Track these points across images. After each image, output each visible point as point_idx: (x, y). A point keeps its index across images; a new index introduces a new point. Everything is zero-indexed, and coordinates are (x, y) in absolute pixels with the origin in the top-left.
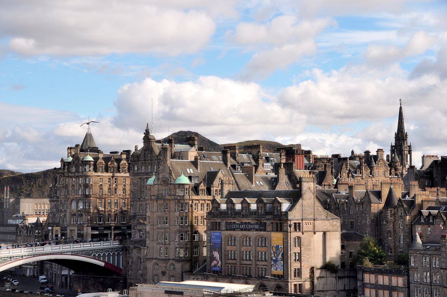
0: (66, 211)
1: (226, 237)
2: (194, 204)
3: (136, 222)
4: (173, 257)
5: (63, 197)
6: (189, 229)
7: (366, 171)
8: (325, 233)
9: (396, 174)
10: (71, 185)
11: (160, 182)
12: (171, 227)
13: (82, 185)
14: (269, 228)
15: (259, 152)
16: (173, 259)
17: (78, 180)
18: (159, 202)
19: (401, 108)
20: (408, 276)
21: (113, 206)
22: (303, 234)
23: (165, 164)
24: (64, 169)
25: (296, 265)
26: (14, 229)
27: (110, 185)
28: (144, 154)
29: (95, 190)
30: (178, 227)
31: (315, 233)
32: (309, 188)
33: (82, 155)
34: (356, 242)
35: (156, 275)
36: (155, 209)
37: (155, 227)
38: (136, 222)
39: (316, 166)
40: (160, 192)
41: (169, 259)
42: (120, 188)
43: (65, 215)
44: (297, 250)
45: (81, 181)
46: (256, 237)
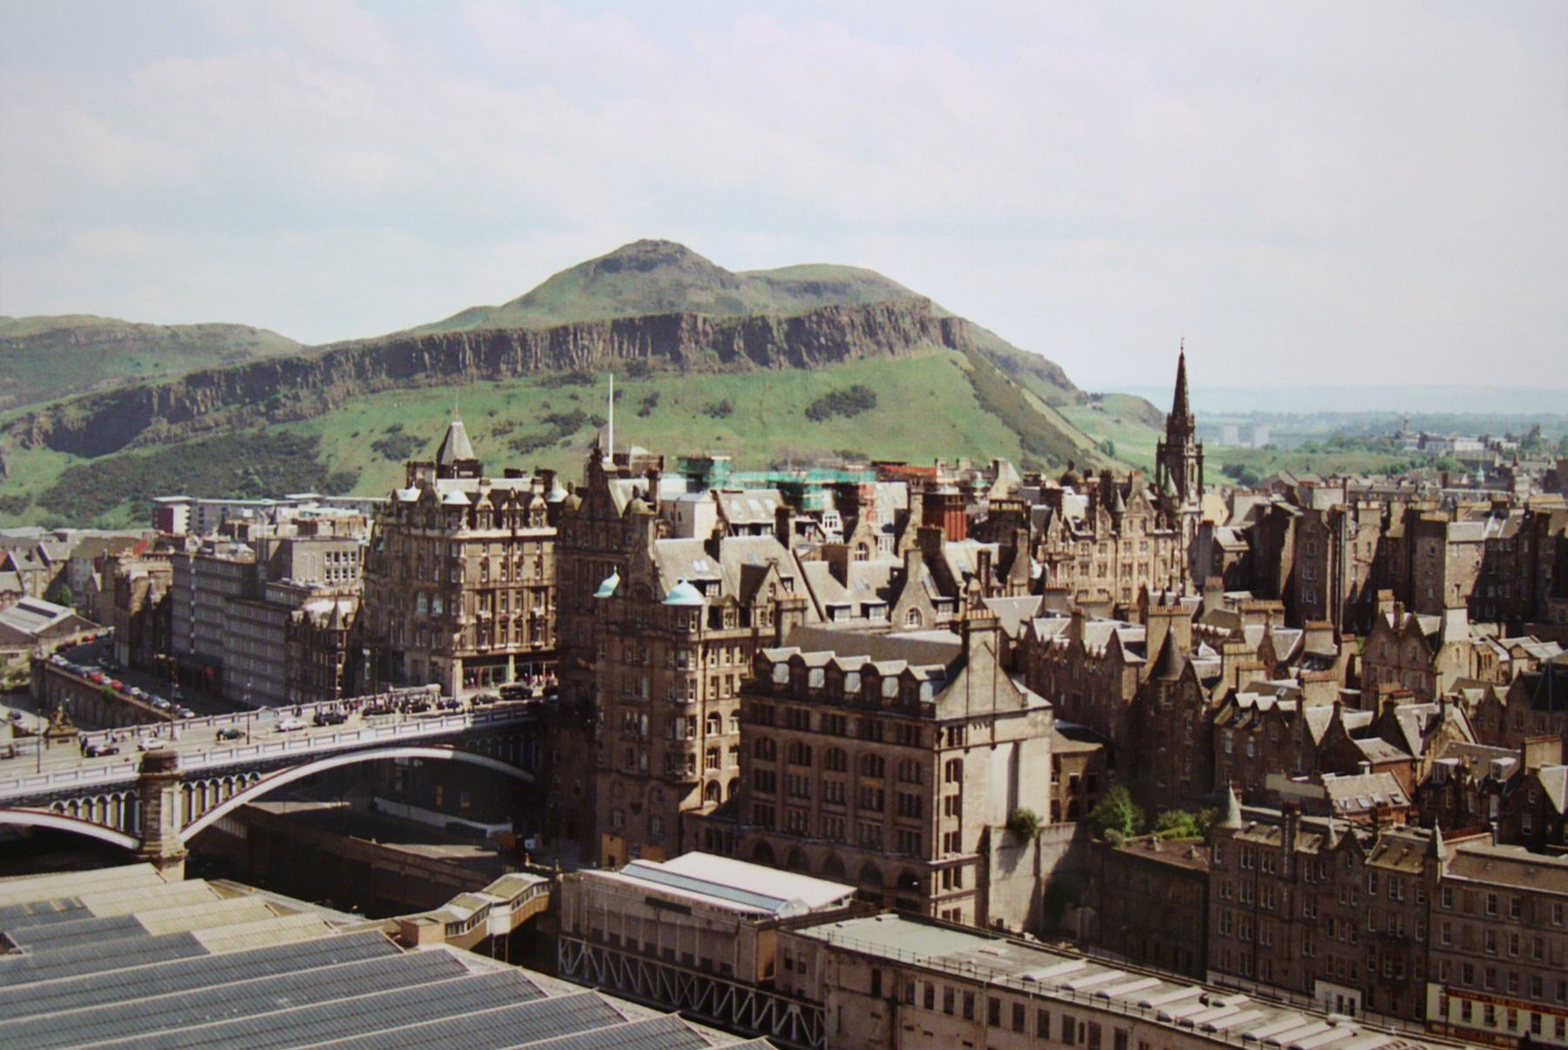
0: (402, 615)
7: (1102, 527)
8: (1017, 744)
9: (1170, 526)
10: (414, 556)
14: (889, 735)
16: (658, 778)
18: (627, 642)
21: (512, 607)
25: (948, 825)
27: (506, 558)
32: (985, 644)
36: (617, 655)
37: (617, 699)
41: (650, 777)
42: (529, 562)
43: (401, 625)
44: (951, 789)
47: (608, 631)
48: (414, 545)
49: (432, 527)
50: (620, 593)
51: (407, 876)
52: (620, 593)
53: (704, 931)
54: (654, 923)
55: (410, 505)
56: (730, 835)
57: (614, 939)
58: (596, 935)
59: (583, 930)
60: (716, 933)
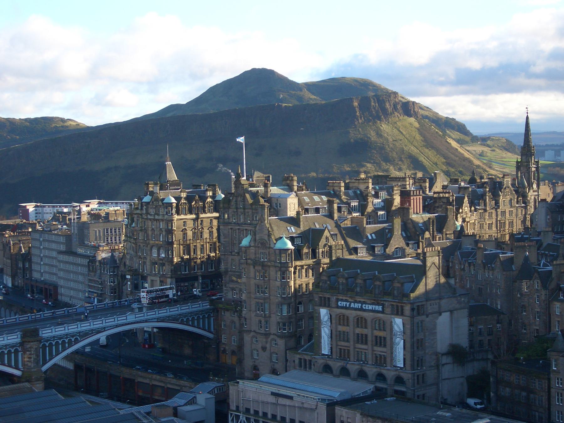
0: (145, 258)
1: (337, 315)
2: (297, 270)
3: (227, 279)
4: (275, 332)
5: (141, 241)
6: (293, 300)
10: (150, 229)
11: (257, 244)
12: (272, 298)
13: (163, 230)
14: (388, 310)
15: (368, 187)
16: (274, 334)
17: (158, 223)
18: (256, 268)
19: (527, 118)
20: (549, 379)
22: (427, 317)
23: (262, 224)
24: (142, 209)
26: (85, 262)
28: (236, 201)
29: (178, 236)
30: (280, 299)
31: (440, 315)
32: (434, 263)
33: (161, 194)
34: (486, 317)
35: (255, 349)
36: (252, 275)
37: (253, 296)
38: (227, 279)
39: (435, 207)
40: (257, 255)
41: (270, 334)
43: (144, 263)
45: (162, 225)
46: (373, 319)
47: (247, 264)
48: (150, 223)
49: (158, 215)
50: (252, 244)
51: (153, 385)
52: (252, 244)
53: (300, 408)
54: (276, 404)
55: (148, 203)
56: (310, 361)
57: (256, 412)
58: (248, 411)
59: (241, 409)
60: (306, 408)
